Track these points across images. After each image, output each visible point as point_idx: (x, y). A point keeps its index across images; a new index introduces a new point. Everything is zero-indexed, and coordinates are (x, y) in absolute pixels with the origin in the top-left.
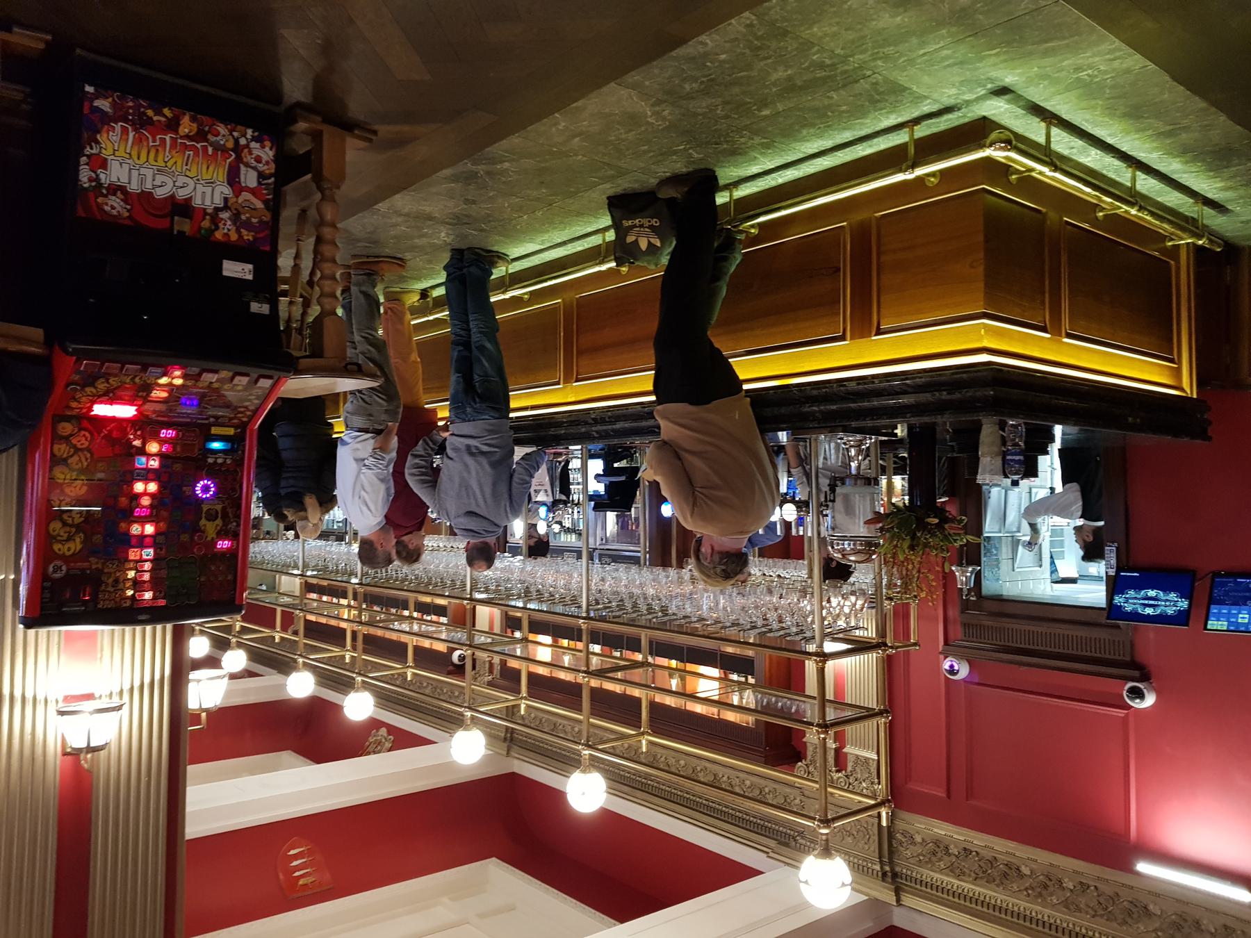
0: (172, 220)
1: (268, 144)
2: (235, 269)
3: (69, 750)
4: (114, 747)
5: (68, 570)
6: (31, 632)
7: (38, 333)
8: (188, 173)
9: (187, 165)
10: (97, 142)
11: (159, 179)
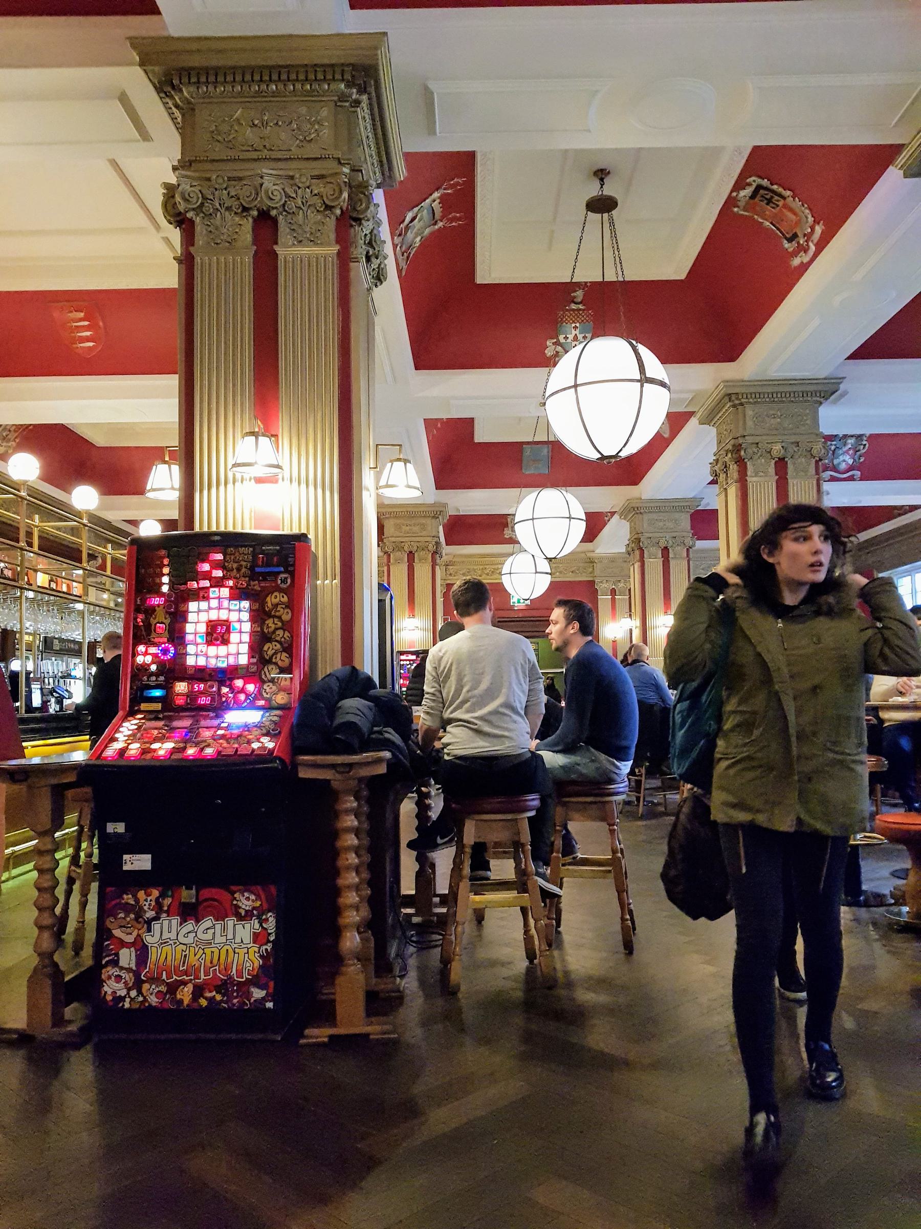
0: (197, 898)
1: (109, 998)
2: (140, 862)
3: (273, 439)
4: (239, 435)
5: (276, 581)
6: (304, 531)
7: (304, 774)
8: (184, 947)
9: (185, 956)
10: (261, 957)
11: (209, 936)
